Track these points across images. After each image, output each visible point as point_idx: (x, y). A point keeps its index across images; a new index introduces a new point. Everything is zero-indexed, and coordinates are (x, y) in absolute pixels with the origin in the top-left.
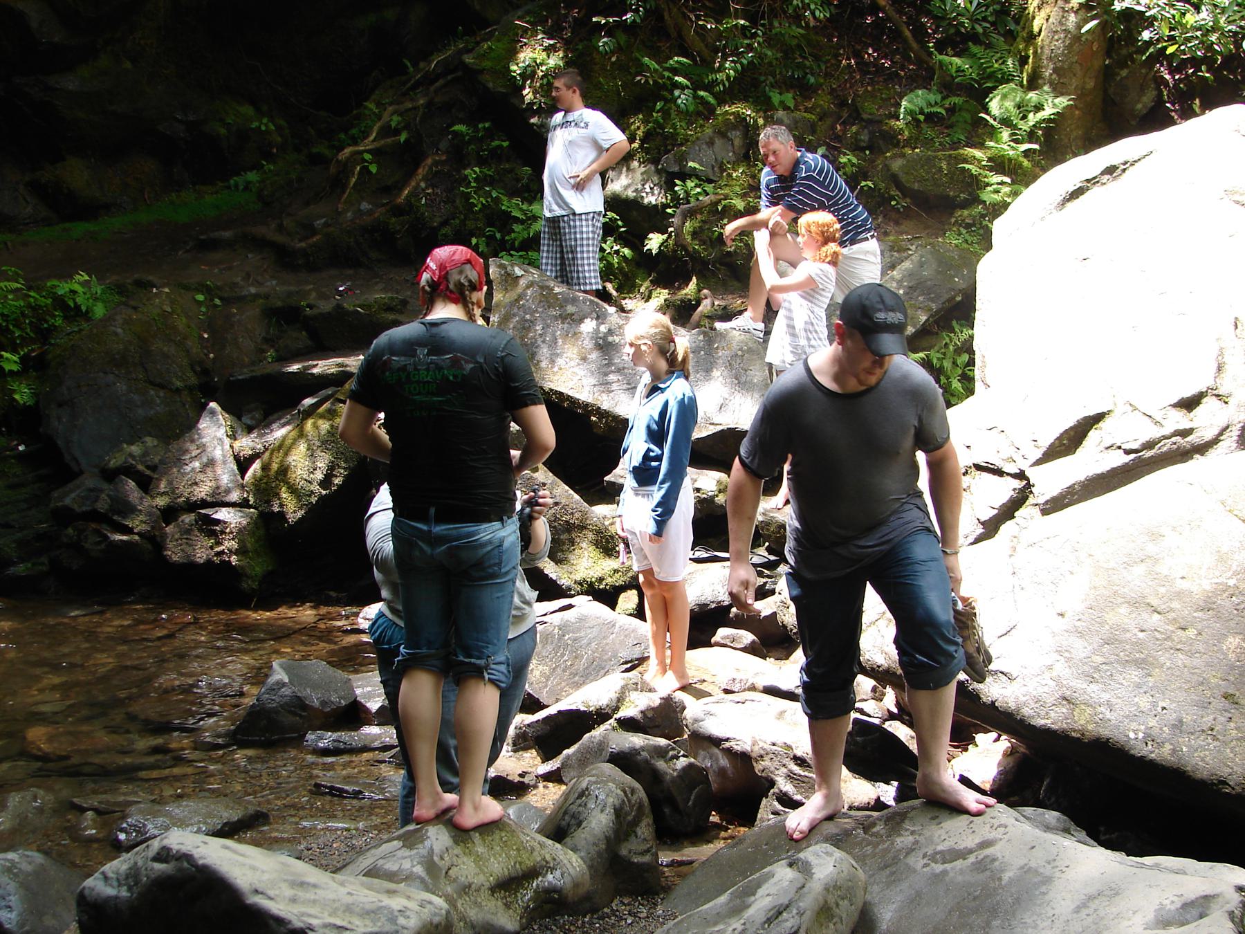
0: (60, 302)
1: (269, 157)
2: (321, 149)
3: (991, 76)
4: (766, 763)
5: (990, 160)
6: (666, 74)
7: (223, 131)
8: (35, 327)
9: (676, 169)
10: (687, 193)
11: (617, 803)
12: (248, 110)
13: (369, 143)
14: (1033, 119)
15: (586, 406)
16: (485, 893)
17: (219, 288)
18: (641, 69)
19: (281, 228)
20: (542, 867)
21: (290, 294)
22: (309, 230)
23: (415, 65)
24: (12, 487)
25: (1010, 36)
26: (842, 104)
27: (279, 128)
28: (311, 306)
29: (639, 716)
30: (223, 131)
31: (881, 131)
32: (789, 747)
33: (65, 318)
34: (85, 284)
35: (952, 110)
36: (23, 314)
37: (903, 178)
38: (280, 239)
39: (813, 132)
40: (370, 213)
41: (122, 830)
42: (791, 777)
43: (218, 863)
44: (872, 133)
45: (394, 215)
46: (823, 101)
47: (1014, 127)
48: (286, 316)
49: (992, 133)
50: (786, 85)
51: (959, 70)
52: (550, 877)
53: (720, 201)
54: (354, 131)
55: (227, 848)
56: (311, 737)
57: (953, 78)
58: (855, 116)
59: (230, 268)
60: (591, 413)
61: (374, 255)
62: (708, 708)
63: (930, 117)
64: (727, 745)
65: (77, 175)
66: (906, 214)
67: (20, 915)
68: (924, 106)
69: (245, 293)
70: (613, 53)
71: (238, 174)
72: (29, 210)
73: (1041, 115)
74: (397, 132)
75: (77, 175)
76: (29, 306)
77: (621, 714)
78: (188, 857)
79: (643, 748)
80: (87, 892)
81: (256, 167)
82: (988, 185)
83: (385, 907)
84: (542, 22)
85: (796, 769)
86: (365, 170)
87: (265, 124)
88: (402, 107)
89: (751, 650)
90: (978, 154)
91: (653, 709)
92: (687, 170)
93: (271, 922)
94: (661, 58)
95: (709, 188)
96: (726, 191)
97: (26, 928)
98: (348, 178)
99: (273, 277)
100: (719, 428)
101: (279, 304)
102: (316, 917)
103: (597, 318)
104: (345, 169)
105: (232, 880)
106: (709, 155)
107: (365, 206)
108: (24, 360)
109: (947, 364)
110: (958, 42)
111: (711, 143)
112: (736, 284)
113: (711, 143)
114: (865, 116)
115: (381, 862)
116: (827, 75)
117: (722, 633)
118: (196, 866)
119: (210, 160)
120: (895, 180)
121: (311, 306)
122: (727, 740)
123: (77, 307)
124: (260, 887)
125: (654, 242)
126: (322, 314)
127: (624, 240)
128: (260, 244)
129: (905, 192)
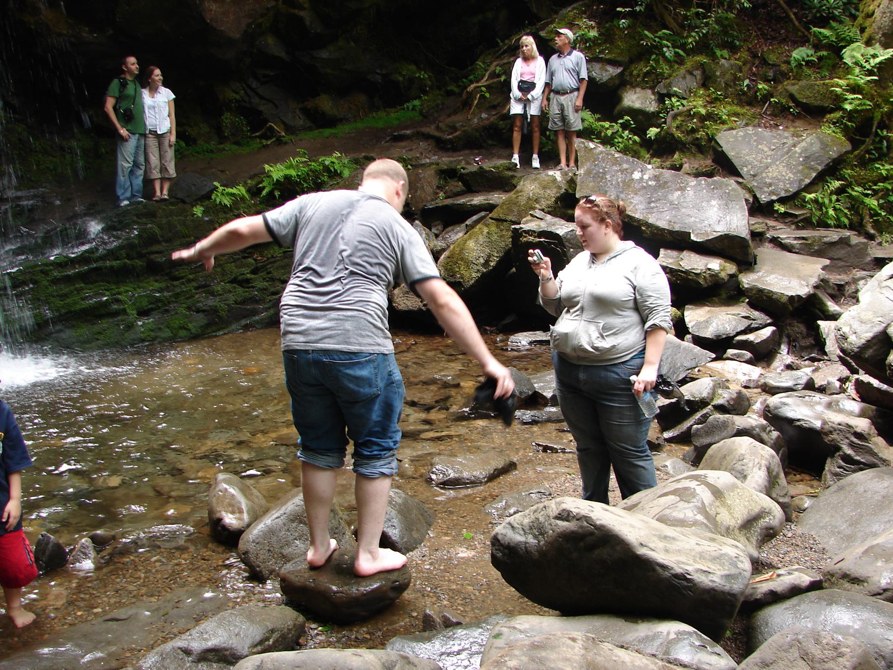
0: (327, 169)
1: (425, 92)
2: (452, 87)
3: (843, 39)
4: (834, 436)
5: (848, 86)
6: (657, 40)
7: (401, 79)
8: (315, 183)
9: (665, 92)
10: (673, 106)
11: (767, 463)
12: (413, 67)
13: (483, 82)
14: (873, 62)
15: (639, 221)
16: (737, 532)
17: (409, 159)
18: (643, 37)
19: (438, 128)
20: (762, 512)
21: (451, 162)
22: (454, 129)
23: (503, 41)
25: (854, 18)
26: (754, 56)
27: (430, 77)
28: (464, 168)
29: (726, 404)
30: (401, 79)
31: (780, 71)
32: (850, 427)
33: (329, 177)
34: (338, 158)
35: (820, 59)
36: (308, 174)
37: (798, 96)
38: (437, 134)
39: (741, 72)
40: (488, 119)
41: (433, 473)
42: (852, 445)
43: (612, 523)
44: (775, 72)
45: (502, 120)
46: (744, 55)
47: (862, 67)
48: (449, 174)
49: (848, 70)
50: (723, 46)
51: (826, 37)
52: (767, 520)
53: (692, 109)
54: (472, 77)
55: (607, 510)
56: (518, 413)
57: (821, 41)
58: (764, 62)
59: (411, 150)
60: (642, 225)
61: (490, 142)
62: (784, 400)
63: (808, 63)
64: (798, 423)
65: (325, 104)
66: (798, 117)
67: (401, 531)
68: (805, 56)
69: (423, 162)
70: (626, 29)
71: (408, 102)
72: (301, 122)
73: (878, 60)
74: (499, 76)
75: (325, 104)
76: (311, 170)
77: (715, 402)
78: (587, 518)
79: (756, 426)
80: (500, 537)
81: (419, 98)
82: (846, 99)
83: (725, 554)
84: (585, 13)
85: (855, 440)
86: (483, 97)
87: (423, 75)
88: (502, 62)
89: (749, 362)
90: (841, 82)
91: (733, 399)
92: (672, 92)
93: (658, 568)
94: (654, 32)
95: (684, 102)
96: (695, 103)
97: (405, 540)
98: (473, 101)
99: (434, 155)
100: (719, 234)
101: (445, 167)
102: (687, 564)
103: (642, 171)
104: (471, 95)
105: (624, 537)
106: (683, 84)
107: (484, 115)
109: (826, 201)
110: (823, 22)
111: (684, 78)
112: (701, 156)
113: (684, 78)
114: (771, 62)
115: (667, 512)
116: (745, 41)
117: (731, 352)
118: (595, 526)
119: (393, 95)
120: (792, 97)
121: (464, 168)
122: (799, 420)
123: (336, 171)
124: (643, 540)
125: (653, 132)
126: (471, 172)
127: (634, 131)
128: (427, 137)
129: (798, 103)
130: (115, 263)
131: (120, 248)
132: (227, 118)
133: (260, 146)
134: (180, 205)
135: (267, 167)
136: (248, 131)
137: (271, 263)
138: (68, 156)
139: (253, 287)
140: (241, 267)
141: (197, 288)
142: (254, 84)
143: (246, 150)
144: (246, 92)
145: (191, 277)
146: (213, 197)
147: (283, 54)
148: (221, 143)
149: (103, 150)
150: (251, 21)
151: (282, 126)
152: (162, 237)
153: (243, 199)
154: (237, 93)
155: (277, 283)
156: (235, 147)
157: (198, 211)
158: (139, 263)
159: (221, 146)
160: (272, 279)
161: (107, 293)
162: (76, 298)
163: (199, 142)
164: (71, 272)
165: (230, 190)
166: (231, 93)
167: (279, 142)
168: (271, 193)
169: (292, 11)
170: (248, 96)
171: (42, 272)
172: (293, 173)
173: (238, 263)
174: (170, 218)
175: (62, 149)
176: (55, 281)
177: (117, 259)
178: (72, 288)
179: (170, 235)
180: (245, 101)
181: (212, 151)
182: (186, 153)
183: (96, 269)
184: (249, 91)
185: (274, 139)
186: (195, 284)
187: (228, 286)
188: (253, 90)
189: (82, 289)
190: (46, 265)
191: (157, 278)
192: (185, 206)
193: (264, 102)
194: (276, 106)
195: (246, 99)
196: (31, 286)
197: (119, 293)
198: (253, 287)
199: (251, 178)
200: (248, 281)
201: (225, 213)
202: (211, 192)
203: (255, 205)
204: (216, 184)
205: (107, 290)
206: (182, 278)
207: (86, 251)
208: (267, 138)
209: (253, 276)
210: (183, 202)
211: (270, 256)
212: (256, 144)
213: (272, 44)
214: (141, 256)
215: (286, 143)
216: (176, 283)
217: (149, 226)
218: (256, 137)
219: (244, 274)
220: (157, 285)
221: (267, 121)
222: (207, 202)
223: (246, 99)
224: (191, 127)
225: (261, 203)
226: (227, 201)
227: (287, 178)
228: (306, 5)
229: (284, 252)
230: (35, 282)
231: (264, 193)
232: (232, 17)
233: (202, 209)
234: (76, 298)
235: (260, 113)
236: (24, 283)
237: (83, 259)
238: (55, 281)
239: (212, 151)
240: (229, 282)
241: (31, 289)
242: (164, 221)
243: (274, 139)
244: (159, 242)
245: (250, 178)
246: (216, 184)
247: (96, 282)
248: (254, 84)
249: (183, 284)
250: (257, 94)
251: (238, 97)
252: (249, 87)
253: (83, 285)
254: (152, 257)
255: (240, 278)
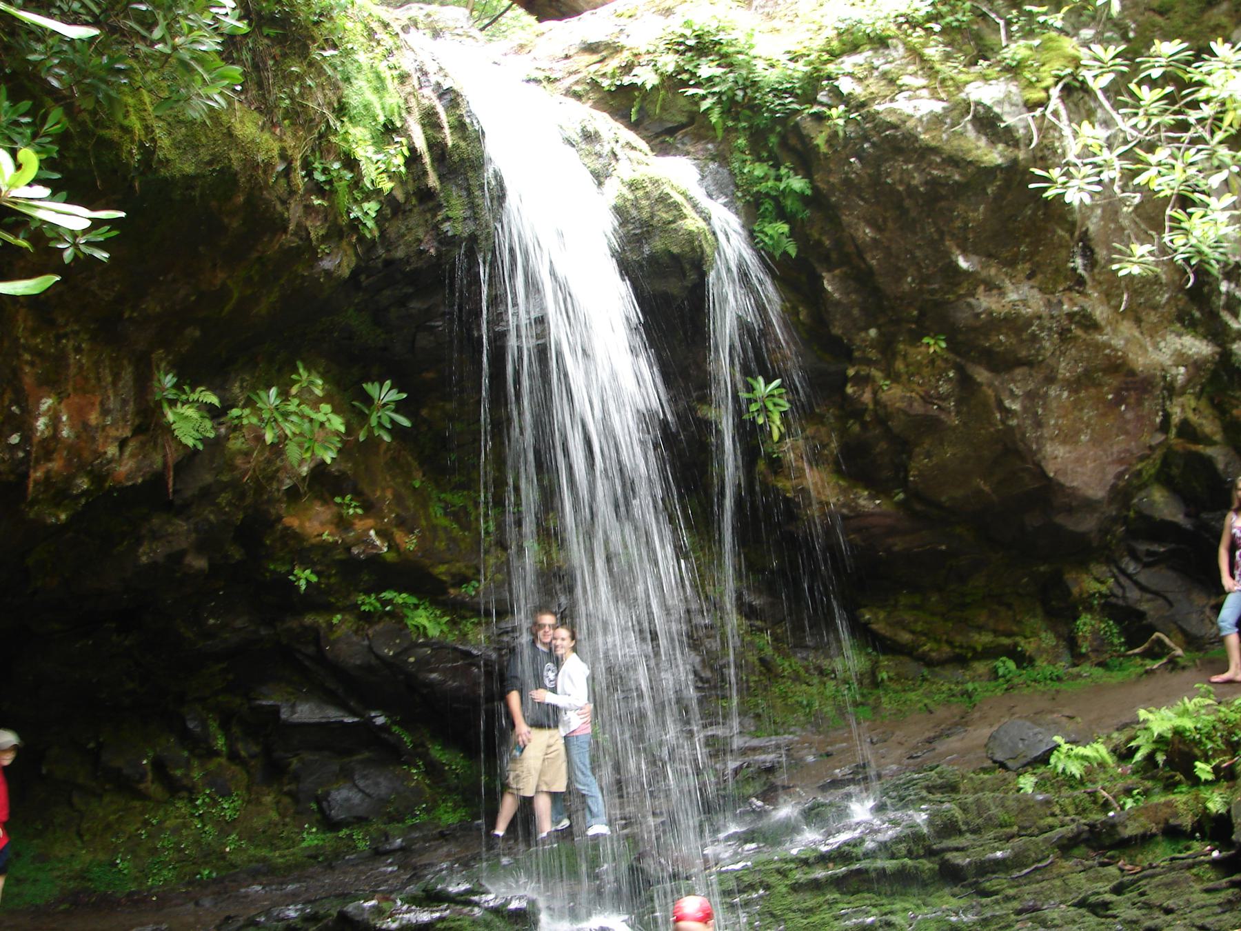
8: (1228, 742)
24: (1207, 891)
36: (1214, 727)
76: (1220, 720)
108: (1216, 770)
130: (889, 865)
131: (898, 840)
132: (1086, 624)
133: (1140, 670)
134: (999, 773)
135: (1143, 714)
136: (1121, 644)
137: (1145, 877)
138: (831, 685)
139: (1115, 917)
140: (1097, 879)
141: (1019, 912)
142: (1132, 568)
143: (1117, 676)
144: (1117, 581)
145: (1011, 892)
146: (1052, 760)
147: (1180, 518)
148: (1075, 665)
149: (885, 675)
150: (1122, 468)
151: (1180, 636)
152: (966, 823)
153: (1102, 765)
154: (1102, 583)
155: (1157, 913)
156: (1099, 671)
157: (1027, 783)
158: (927, 865)
159: (1075, 670)
160: (1148, 906)
161: (874, 911)
162: (827, 916)
163: (1038, 663)
164: (820, 873)
165: (1081, 750)
166: (1091, 582)
167: (1174, 665)
168: (1150, 757)
169: (1194, 448)
170: (1122, 587)
171: (778, 871)
172: (1188, 723)
173: (1091, 873)
174: (980, 794)
175: (821, 672)
176: (796, 888)
177: (893, 856)
178: (821, 899)
179: (980, 821)
180: (1113, 595)
181: (1059, 679)
182: (1016, 681)
183: (859, 871)
184: (1122, 579)
185: (1165, 660)
186: (1016, 905)
187: (1073, 912)
188: (1129, 577)
189: (836, 902)
190: (786, 861)
191: (956, 890)
192: (1007, 774)
193: (1148, 596)
194: (1171, 604)
195: (1119, 592)
196: (761, 892)
197: (892, 913)
198: (1115, 917)
199: (1119, 729)
200: (1106, 905)
201: (1071, 787)
202: (1050, 752)
203: (1123, 775)
204: (1058, 739)
205: (875, 906)
206: (996, 893)
207: (847, 843)
208: (1155, 657)
209: (1114, 898)
210: (1003, 765)
211: (1146, 864)
212: (1134, 669)
213: (1161, 503)
214: (930, 853)
215: (1184, 668)
216: (984, 900)
217: (946, 805)
218: (1135, 655)
219: (1098, 893)
220: (954, 903)
221: (1152, 629)
222: (1041, 769)
223: (1119, 592)
224: (1026, 637)
225: (1134, 773)
226: (1075, 769)
227: (1178, 732)
228: (1218, 438)
229: (1172, 859)
230: (767, 887)
231: (1139, 756)
232: (1090, 465)
233: (1034, 779)
234: (827, 916)
235: (1142, 615)
236: (752, 887)
237: (841, 855)
238: (796, 888)
239: (1059, 679)
240: (1074, 905)
241: (761, 897)
242: (971, 798)
243: (1165, 660)
244: (961, 833)
245: (1118, 730)
246: (1058, 739)
247: (858, 892)
248: (1132, 568)
249: (997, 902)
250: (1136, 583)
251: (1104, 589)
252: (1123, 572)
253: (837, 896)
254: (949, 856)
255: (1092, 899)
